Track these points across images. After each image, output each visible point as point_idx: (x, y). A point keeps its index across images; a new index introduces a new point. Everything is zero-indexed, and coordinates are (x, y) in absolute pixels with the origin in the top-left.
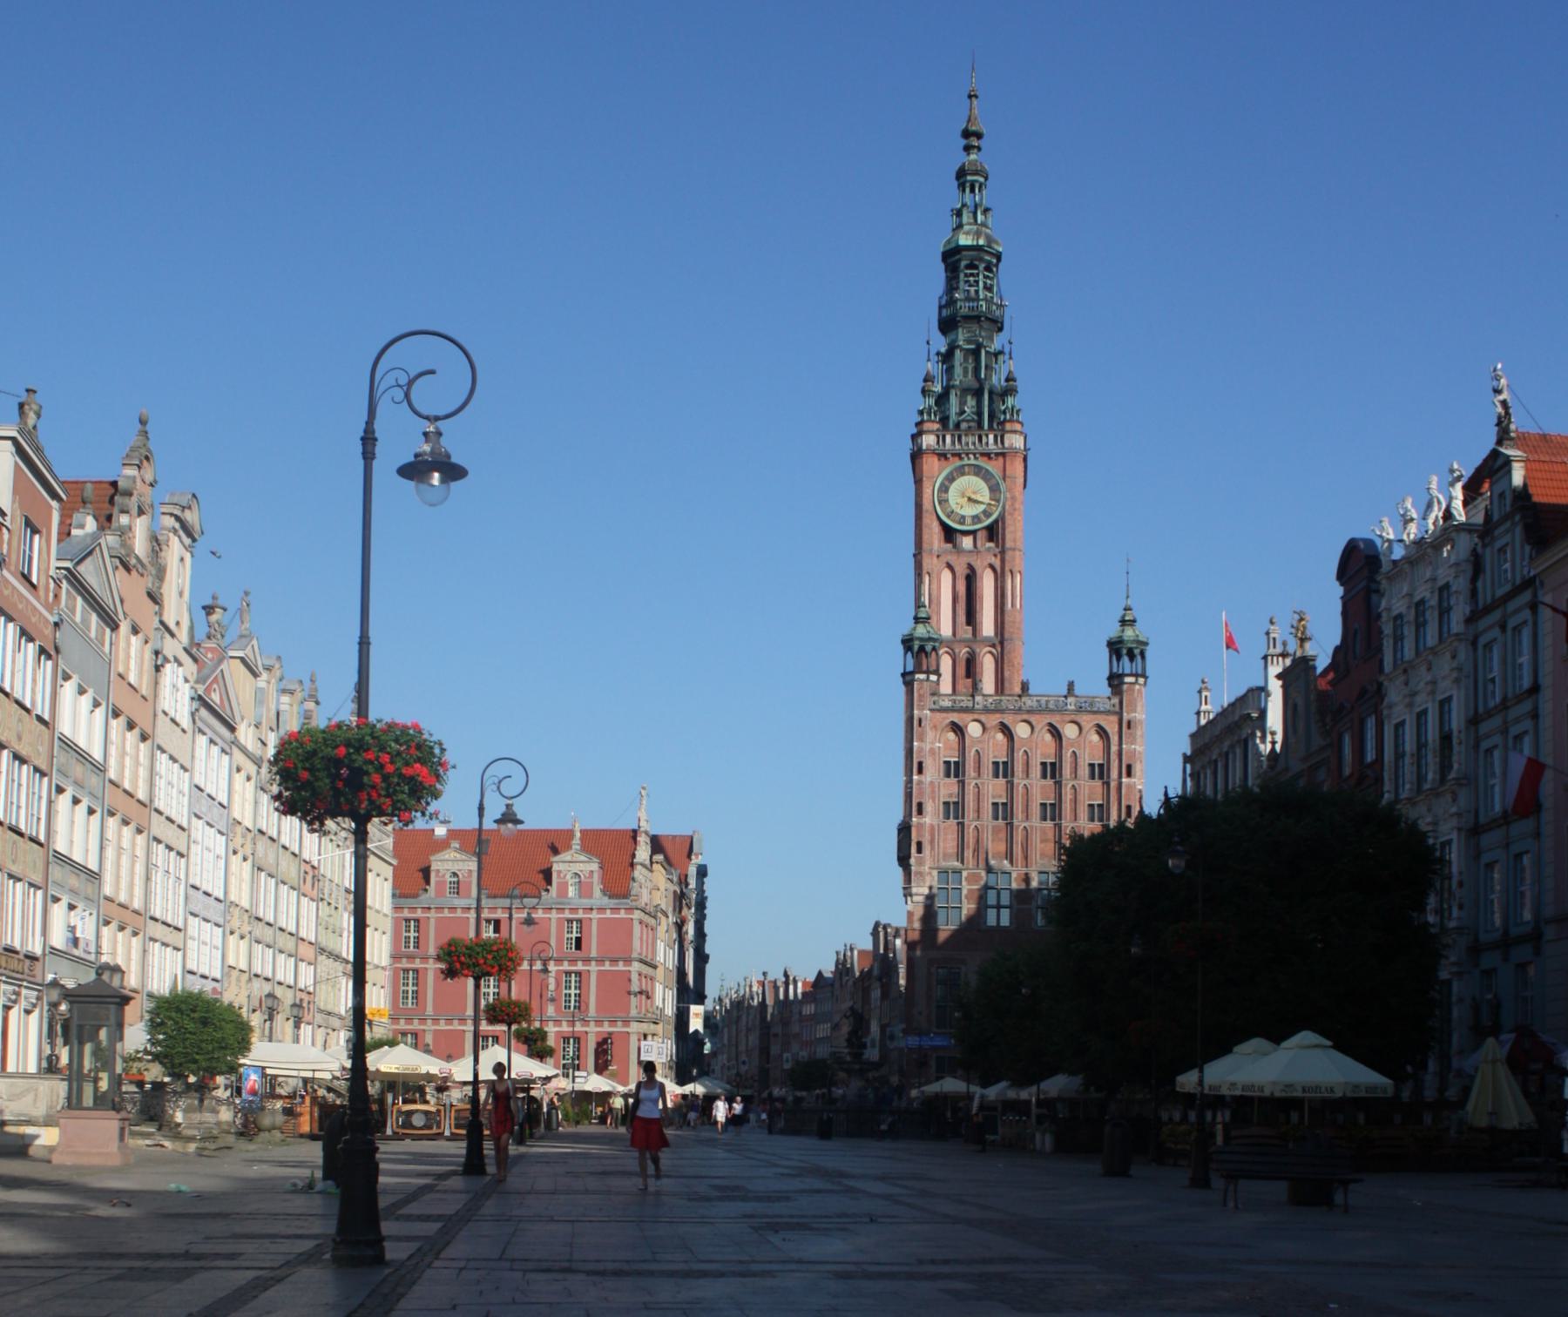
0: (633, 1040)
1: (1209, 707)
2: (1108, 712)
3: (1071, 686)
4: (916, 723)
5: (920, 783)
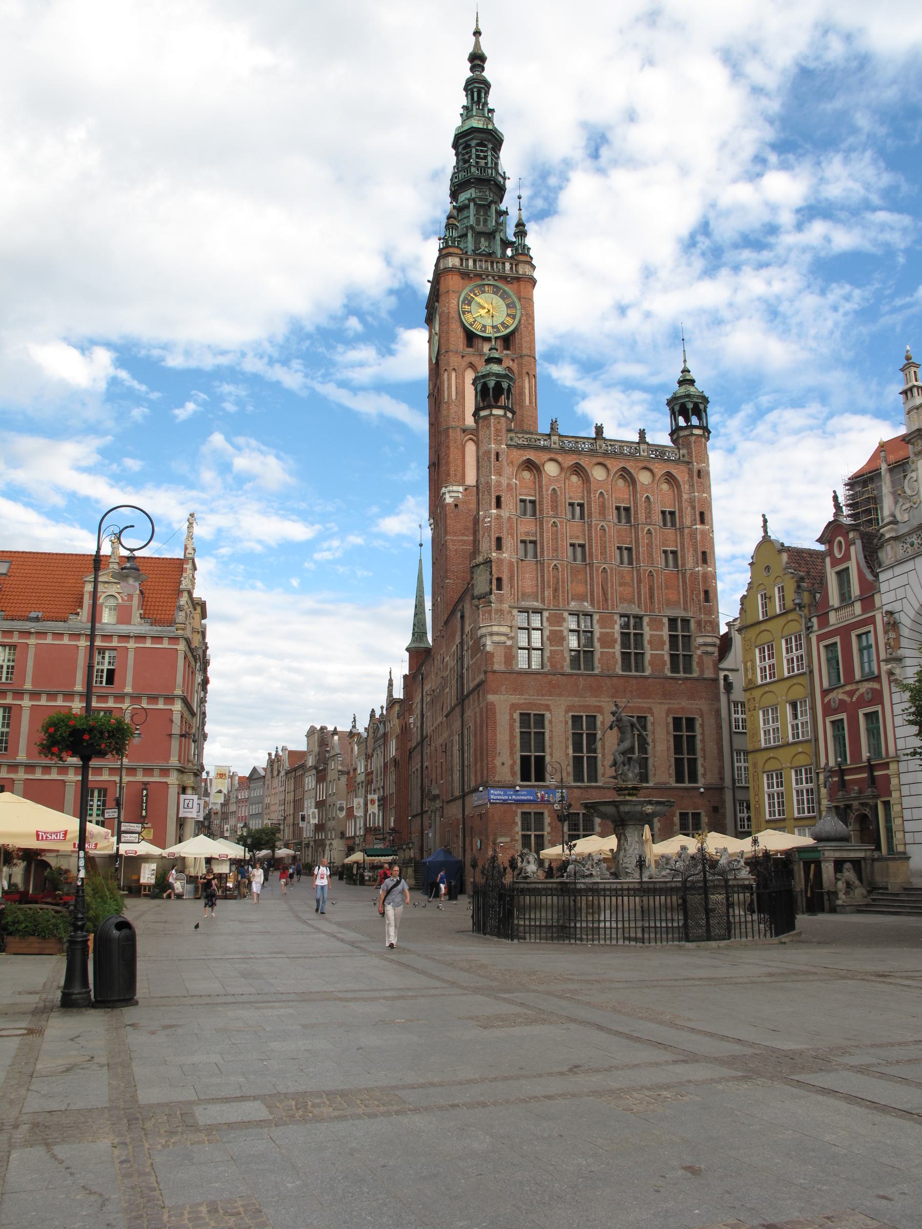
0: (173, 791)
3: (642, 433)
5: (499, 517)
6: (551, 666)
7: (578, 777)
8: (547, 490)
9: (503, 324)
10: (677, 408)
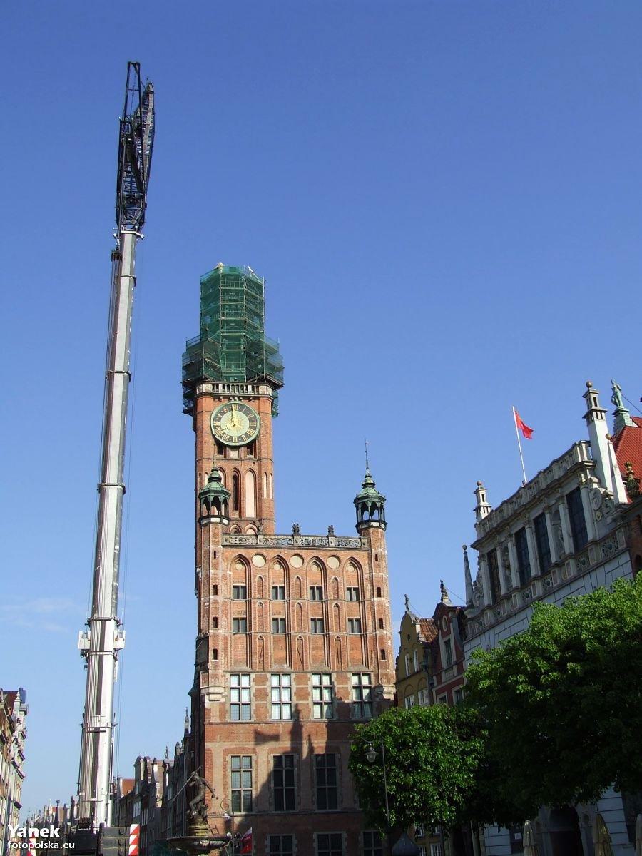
1: (486, 503)
2: (360, 549)
3: (331, 529)
4: (212, 555)
5: (216, 601)
6: (257, 717)
7: (278, 806)
8: (254, 578)
9: (246, 434)
10: (360, 506)
